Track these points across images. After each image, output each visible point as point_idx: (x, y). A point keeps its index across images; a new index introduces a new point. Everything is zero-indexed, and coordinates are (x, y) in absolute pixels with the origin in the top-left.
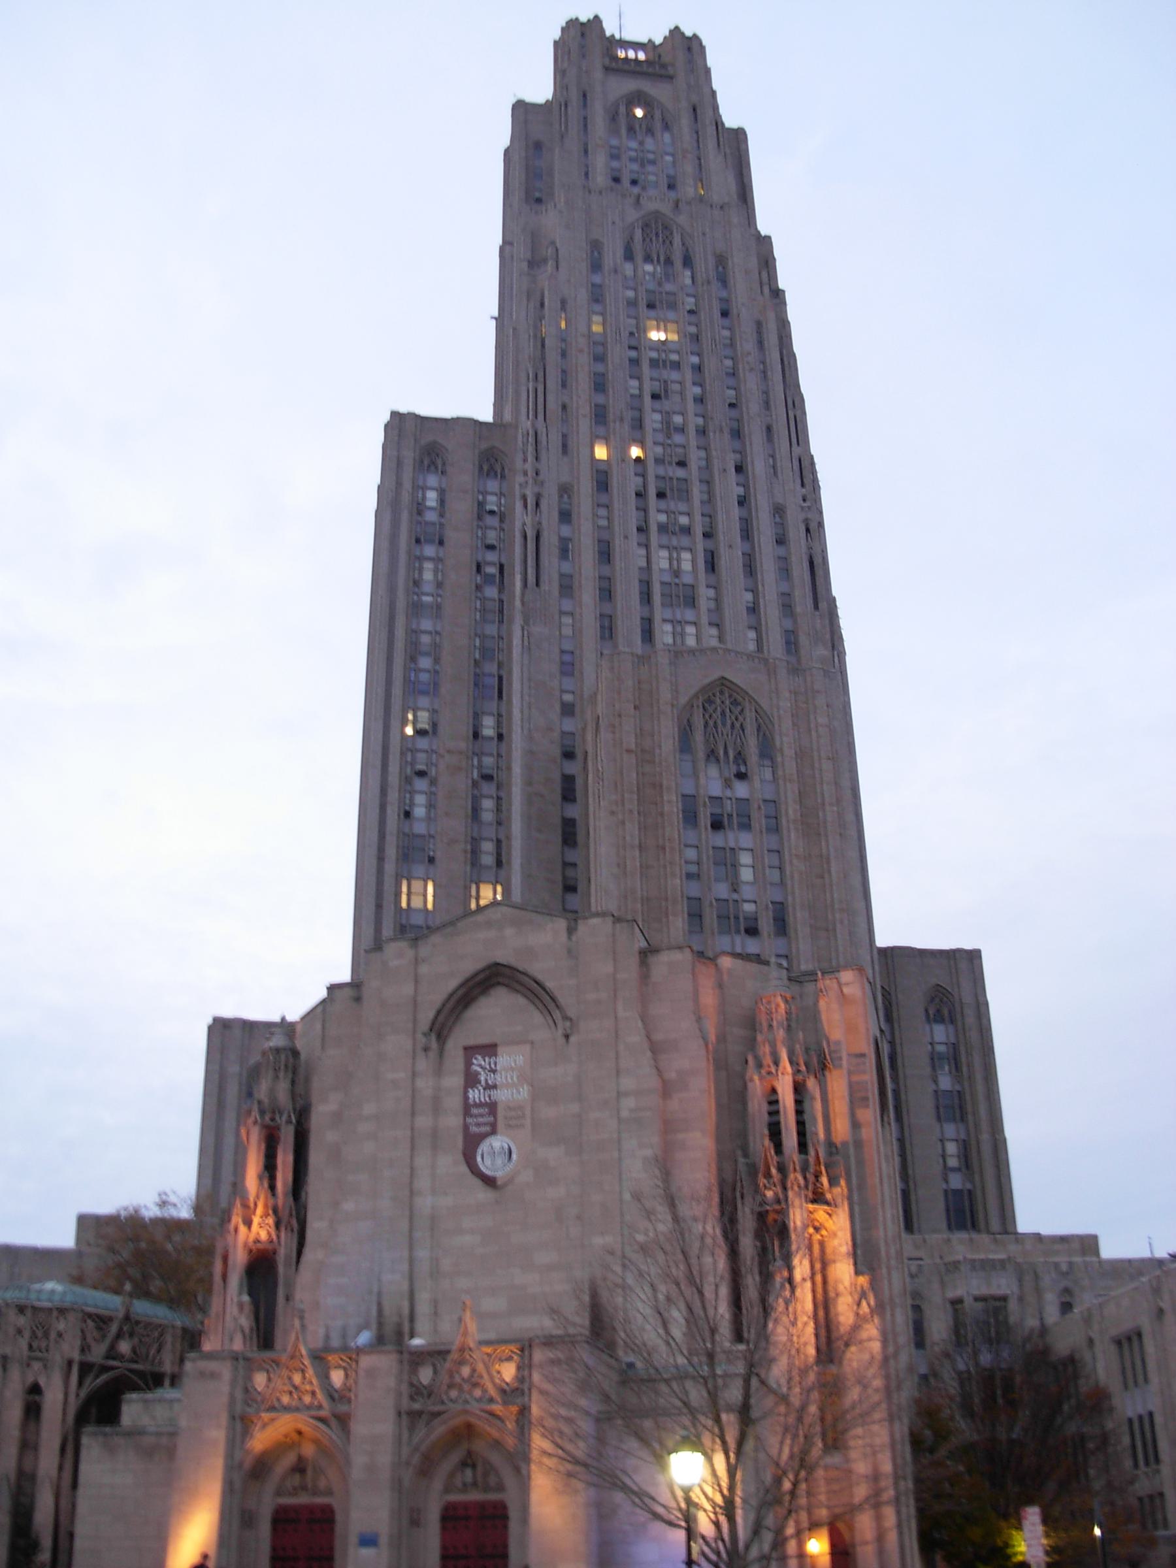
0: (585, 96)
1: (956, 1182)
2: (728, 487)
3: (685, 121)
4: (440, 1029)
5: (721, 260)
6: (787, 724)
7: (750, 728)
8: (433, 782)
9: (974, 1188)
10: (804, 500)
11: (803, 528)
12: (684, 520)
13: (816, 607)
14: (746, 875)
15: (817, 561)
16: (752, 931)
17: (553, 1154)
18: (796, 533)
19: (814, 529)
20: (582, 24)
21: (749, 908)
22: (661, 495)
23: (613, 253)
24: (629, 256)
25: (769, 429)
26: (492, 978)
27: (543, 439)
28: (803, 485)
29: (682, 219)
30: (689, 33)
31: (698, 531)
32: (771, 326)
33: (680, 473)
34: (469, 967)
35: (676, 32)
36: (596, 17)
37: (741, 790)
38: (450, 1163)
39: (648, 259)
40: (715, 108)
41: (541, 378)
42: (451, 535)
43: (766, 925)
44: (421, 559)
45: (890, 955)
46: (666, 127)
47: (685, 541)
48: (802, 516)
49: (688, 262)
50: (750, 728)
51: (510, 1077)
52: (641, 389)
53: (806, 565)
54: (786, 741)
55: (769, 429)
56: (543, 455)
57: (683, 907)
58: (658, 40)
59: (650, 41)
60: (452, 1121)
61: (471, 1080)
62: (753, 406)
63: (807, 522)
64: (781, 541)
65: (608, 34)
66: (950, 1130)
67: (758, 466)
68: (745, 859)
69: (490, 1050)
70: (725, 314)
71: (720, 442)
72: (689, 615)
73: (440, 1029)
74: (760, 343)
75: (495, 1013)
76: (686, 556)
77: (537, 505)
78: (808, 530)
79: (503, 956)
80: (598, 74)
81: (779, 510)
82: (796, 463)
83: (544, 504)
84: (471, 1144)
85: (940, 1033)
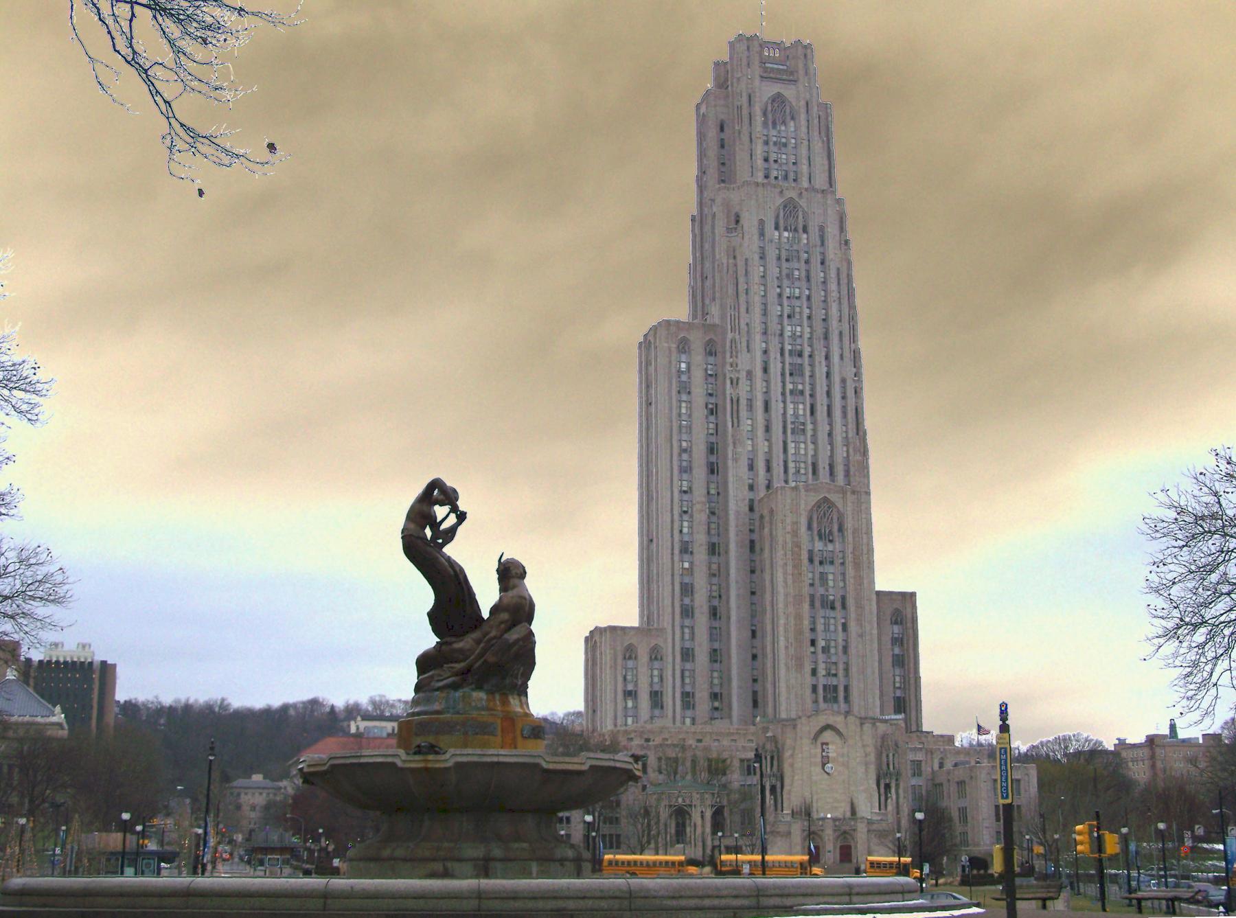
1: (899, 693)
2: (821, 370)
3: (803, 116)
4: (816, 738)
5: (822, 229)
6: (850, 518)
7: (835, 520)
8: (691, 516)
9: (905, 699)
12: (800, 387)
14: (831, 583)
16: (833, 608)
17: (841, 768)
19: (857, 392)
21: (831, 598)
22: (791, 374)
23: (770, 226)
24: (777, 228)
25: (841, 333)
26: (827, 727)
29: (803, 203)
31: (807, 393)
33: (799, 361)
34: (822, 724)
37: (830, 547)
38: (819, 769)
39: (786, 229)
42: (693, 390)
43: (838, 605)
44: (680, 401)
45: (878, 593)
46: (793, 118)
47: (801, 399)
49: (805, 230)
50: (835, 520)
51: (832, 751)
52: (782, 311)
54: (849, 524)
55: (841, 333)
57: (808, 599)
60: (819, 760)
61: (823, 750)
62: (834, 323)
64: (844, 398)
66: (898, 671)
67: (835, 358)
68: (831, 577)
69: (827, 744)
70: (822, 263)
71: (819, 346)
72: (802, 438)
73: (816, 738)
74: (839, 284)
75: (828, 736)
76: (801, 406)
79: (830, 722)
80: (757, 82)
81: (843, 381)
84: (824, 765)
85: (896, 629)
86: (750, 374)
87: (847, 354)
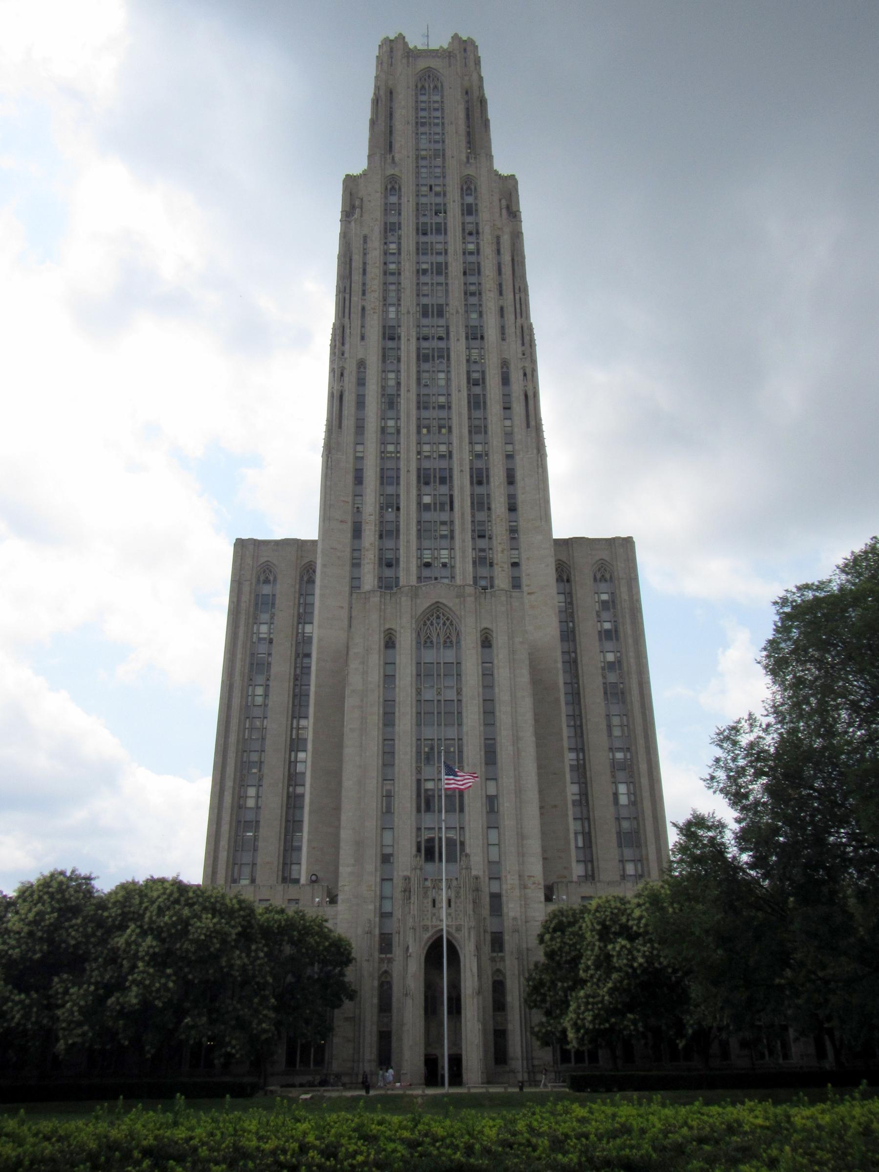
0: (391, 93)
10: (524, 354)
11: (521, 373)
13: (528, 426)
15: (530, 394)
18: (516, 377)
20: (391, 41)
25: (502, 309)
27: (347, 331)
28: (523, 344)
30: (465, 38)
32: (506, 240)
35: (456, 37)
36: (400, 34)
40: (481, 88)
41: (348, 291)
48: (520, 365)
53: (522, 398)
55: (502, 309)
56: (347, 339)
58: (445, 46)
59: (441, 47)
63: (524, 368)
65: (411, 46)
77: (342, 375)
78: (525, 375)
81: (505, 364)
82: (519, 331)
83: (346, 374)
86: (362, 364)
87: (511, 330)
